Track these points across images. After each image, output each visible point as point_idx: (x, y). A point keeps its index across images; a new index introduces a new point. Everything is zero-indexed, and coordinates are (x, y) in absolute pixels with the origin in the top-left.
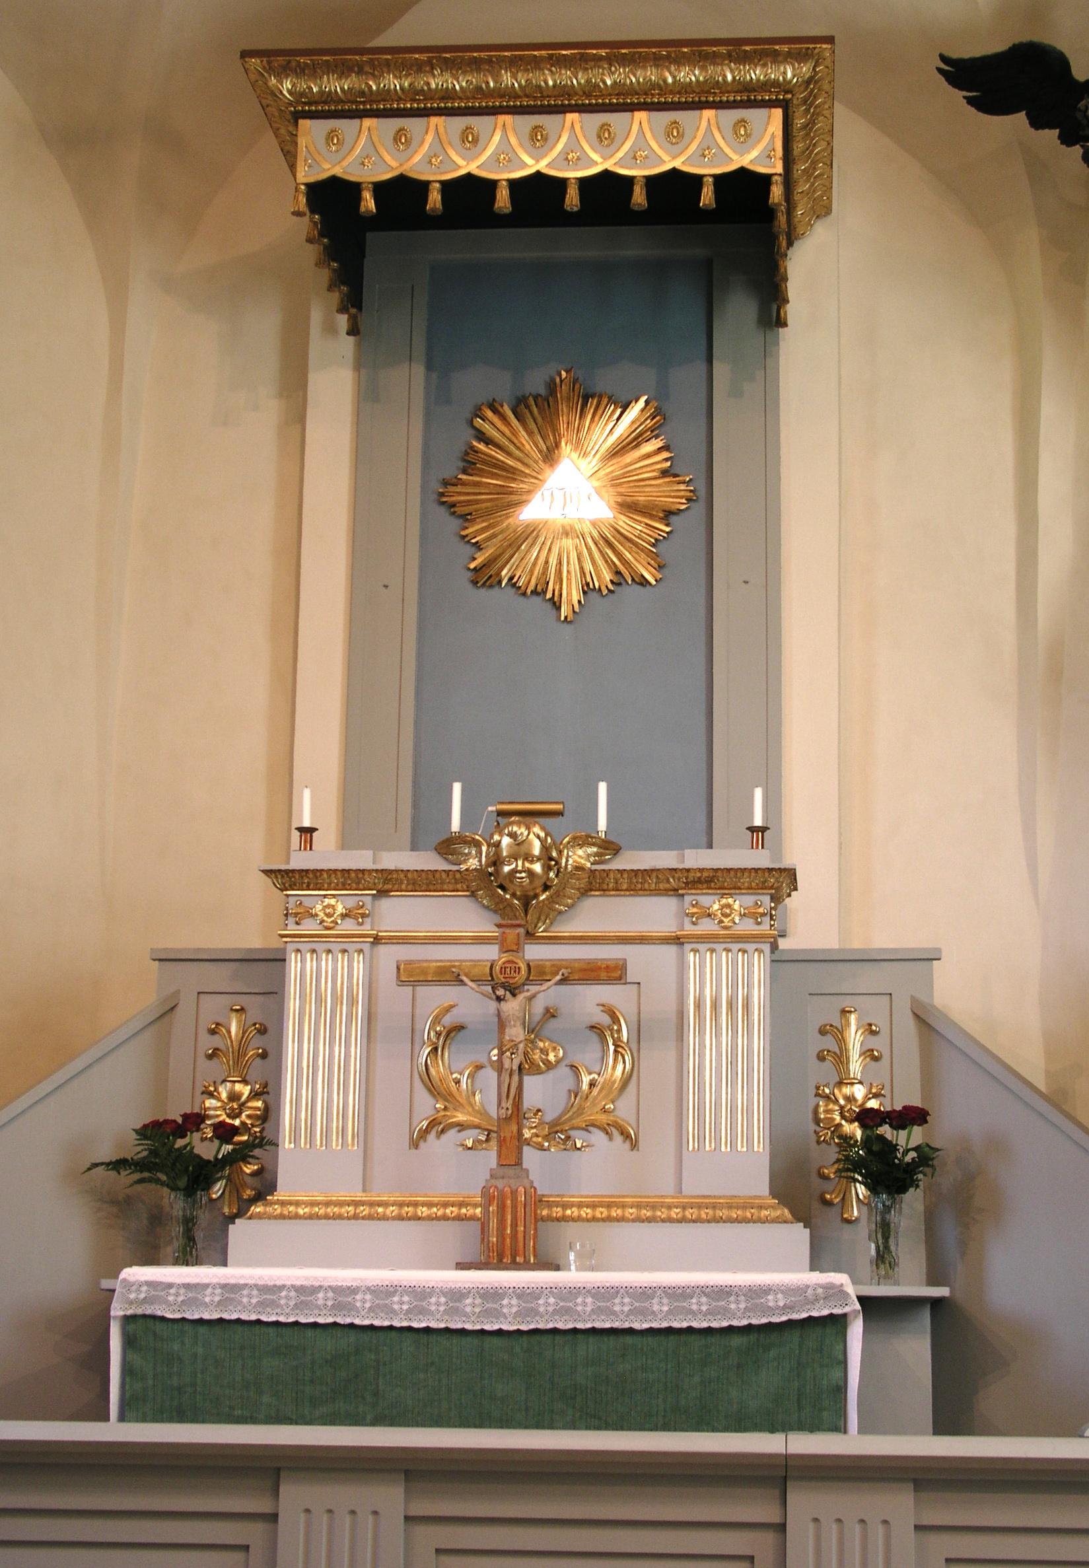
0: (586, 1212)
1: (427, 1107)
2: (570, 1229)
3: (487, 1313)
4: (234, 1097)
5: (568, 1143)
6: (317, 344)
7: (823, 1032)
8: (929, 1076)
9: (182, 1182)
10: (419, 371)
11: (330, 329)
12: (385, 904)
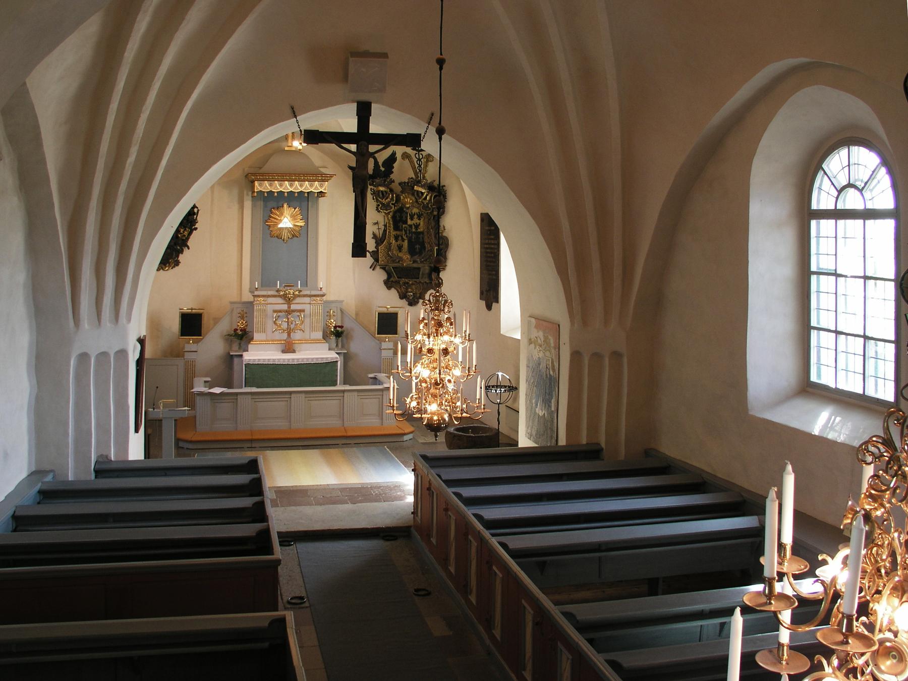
0: (298, 342)
1: (275, 327)
2: (296, 345)
3: (293, 362)
4: (242, 323)
5: (295, 332)
6: (246, 197)
7: (327, 312)
8: (342, 321)
9: (239, 338)
10: (262, 203)
11: (248, 195)
12: (268, 299)
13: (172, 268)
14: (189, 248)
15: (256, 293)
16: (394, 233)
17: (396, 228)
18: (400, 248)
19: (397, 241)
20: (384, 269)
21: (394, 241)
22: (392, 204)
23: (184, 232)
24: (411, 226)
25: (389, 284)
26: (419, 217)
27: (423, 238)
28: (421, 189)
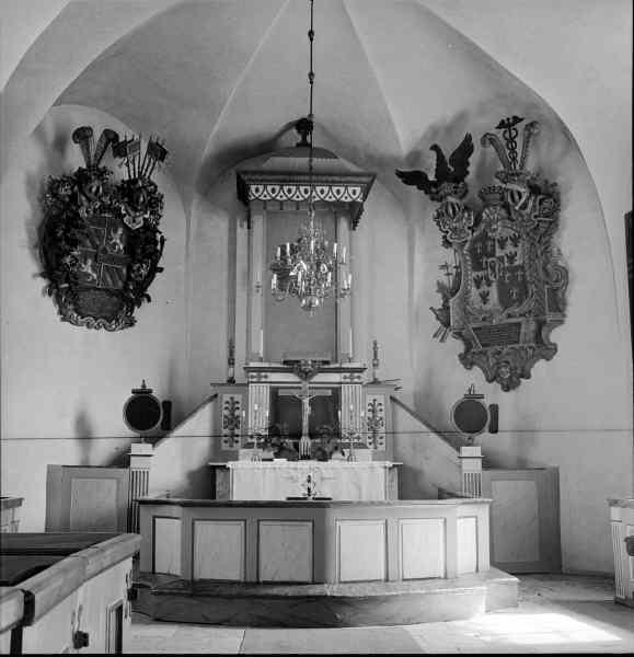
6: (239, 230)
13: (122, 329)
14: (149, 300)
15: (252, 365)
16: (474, 274)
17: (477, 266)
18: (484, 297)
19: (478, 287)
20: (459, 335)
21: (474, 289)
22: (469, 228)
23: (139, 269)
24: (501, 259)
25: (467, 360)
26: (515, 241)
27: (523, 276)
28: (515, 187)
